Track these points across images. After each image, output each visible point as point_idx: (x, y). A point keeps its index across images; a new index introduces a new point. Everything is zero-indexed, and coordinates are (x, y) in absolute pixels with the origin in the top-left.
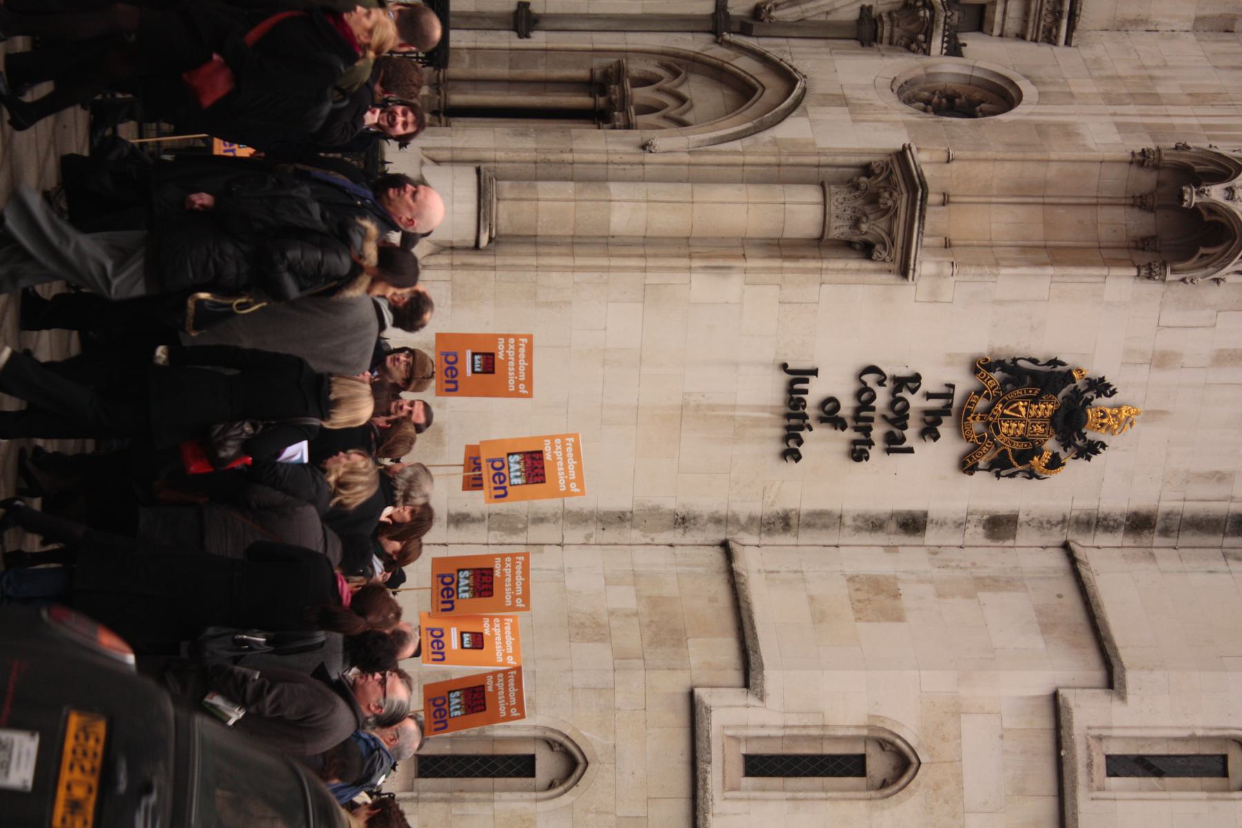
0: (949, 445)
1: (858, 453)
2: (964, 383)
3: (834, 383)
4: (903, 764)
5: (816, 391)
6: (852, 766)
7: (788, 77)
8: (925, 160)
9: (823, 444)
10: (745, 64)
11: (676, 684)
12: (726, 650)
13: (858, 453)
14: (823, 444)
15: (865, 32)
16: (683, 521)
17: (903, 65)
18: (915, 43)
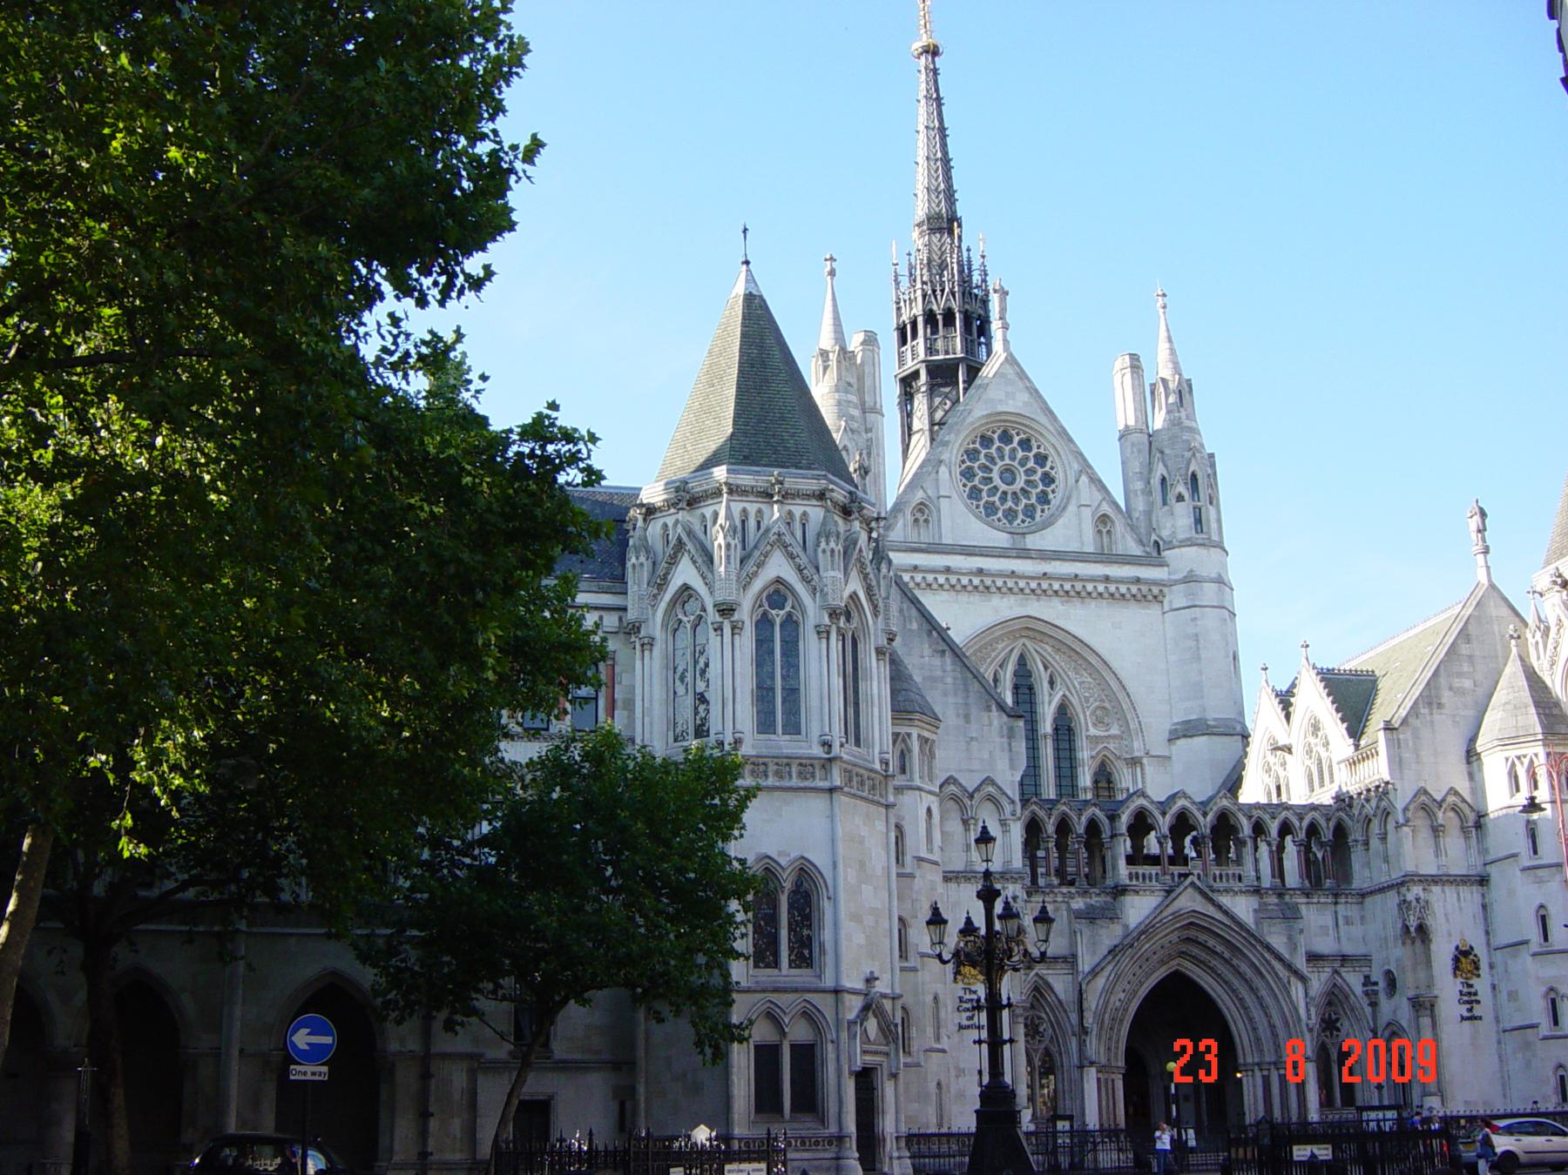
0: (1473, 981)
1: (1478, 1002)
2: (1460, 980)
3: (1463, 1010)
4: (1552, 989)
5: (1466, 1014)
6: (1553, 1001)
7: (1389, 1024)
8: (1411, 993)
9: (1477, 1011)
10: (1386, 1034)
11: (1539, 1044)
12: (1529, 1031)
13: (1478, 1002)
14: (1476, 1013)
15: (1374, 1005)
16: (1499, 1042)
17: (1382, 998)
18: (1376, 993)
